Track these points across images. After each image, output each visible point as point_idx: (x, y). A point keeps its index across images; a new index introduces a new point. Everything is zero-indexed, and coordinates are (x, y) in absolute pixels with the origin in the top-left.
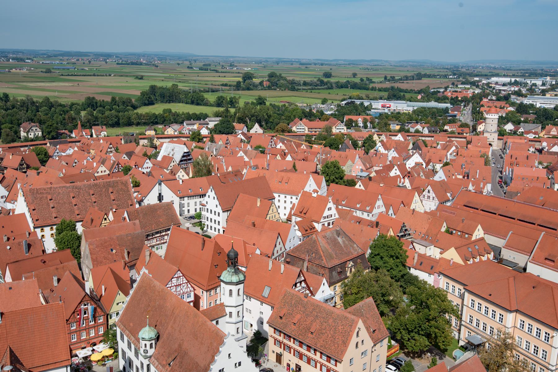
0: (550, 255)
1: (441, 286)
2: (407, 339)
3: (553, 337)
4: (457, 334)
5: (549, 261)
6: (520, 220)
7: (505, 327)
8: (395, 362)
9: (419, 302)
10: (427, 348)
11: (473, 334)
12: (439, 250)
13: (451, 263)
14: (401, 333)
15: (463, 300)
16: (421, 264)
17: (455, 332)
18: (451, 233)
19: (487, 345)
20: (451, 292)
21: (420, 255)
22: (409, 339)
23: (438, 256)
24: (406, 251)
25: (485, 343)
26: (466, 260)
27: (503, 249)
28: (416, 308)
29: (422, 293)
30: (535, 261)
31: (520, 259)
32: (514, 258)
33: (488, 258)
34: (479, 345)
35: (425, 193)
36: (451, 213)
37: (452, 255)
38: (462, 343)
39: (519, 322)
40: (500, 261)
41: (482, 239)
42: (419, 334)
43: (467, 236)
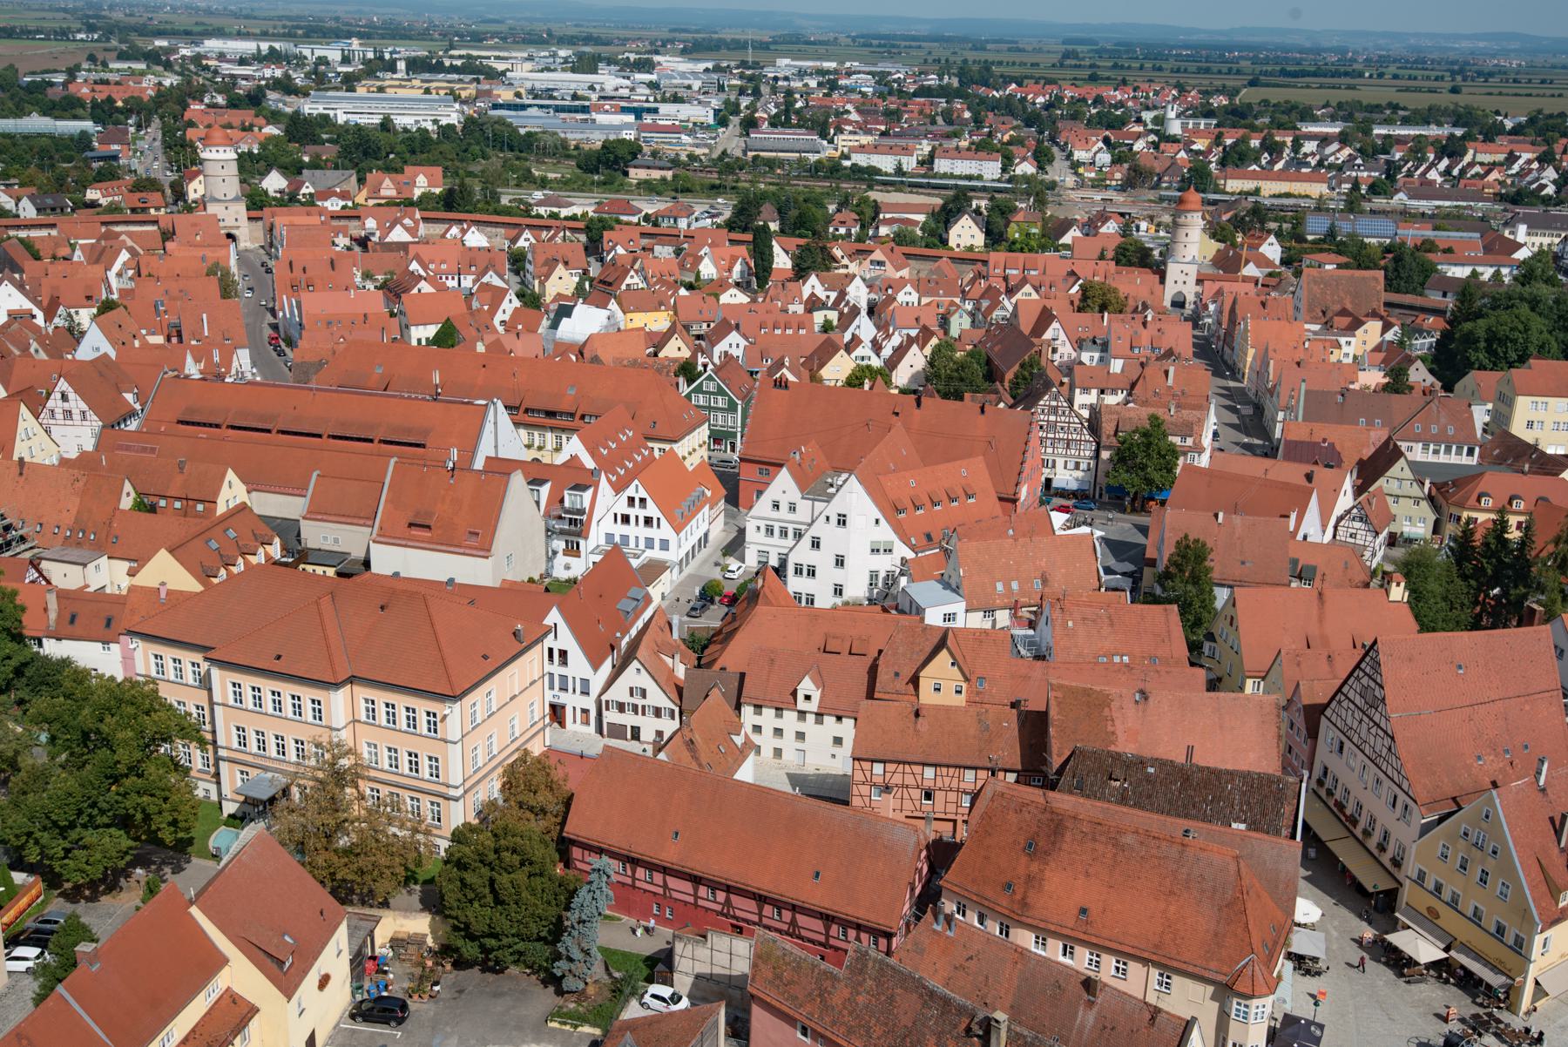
0: (417, 515)
1: (140, 669)
2: (62, 854)
3: (445, 717)
4: (213, 788)
5: (419, 528)
6: (334, 437)
7: (331, 729)
8: (37, 931)
9: (77, 735)
10: (128, 858)
11: (253, 773)
12: (125, 565)
13: (163, 595)
14: (37, 842)
15: (210, 690)
16: (72, 621)
17: (200, 784)
18: (153, 509)
19: (295, 791)
20: (172, 678)
21: (63, 595)
22: (67, 851)
23: (125, 582)
24: (14, 593)
25: (286, 792)
26: (205, 575)
27: (303, 523)
28: (72, 754)
29: (80, 708)
30: (387, 537)
31: (348, 539)
32: (336, 541)
33: (268, 557)
34: (272, 800)
35: (54, 402)
36: (144, 450)
37: (167, 572)
38: (230, 808)
39: (363, 705)
40: (299, 554)
41: (243, 508)
42: (97, 827)
43: (200, 507)
